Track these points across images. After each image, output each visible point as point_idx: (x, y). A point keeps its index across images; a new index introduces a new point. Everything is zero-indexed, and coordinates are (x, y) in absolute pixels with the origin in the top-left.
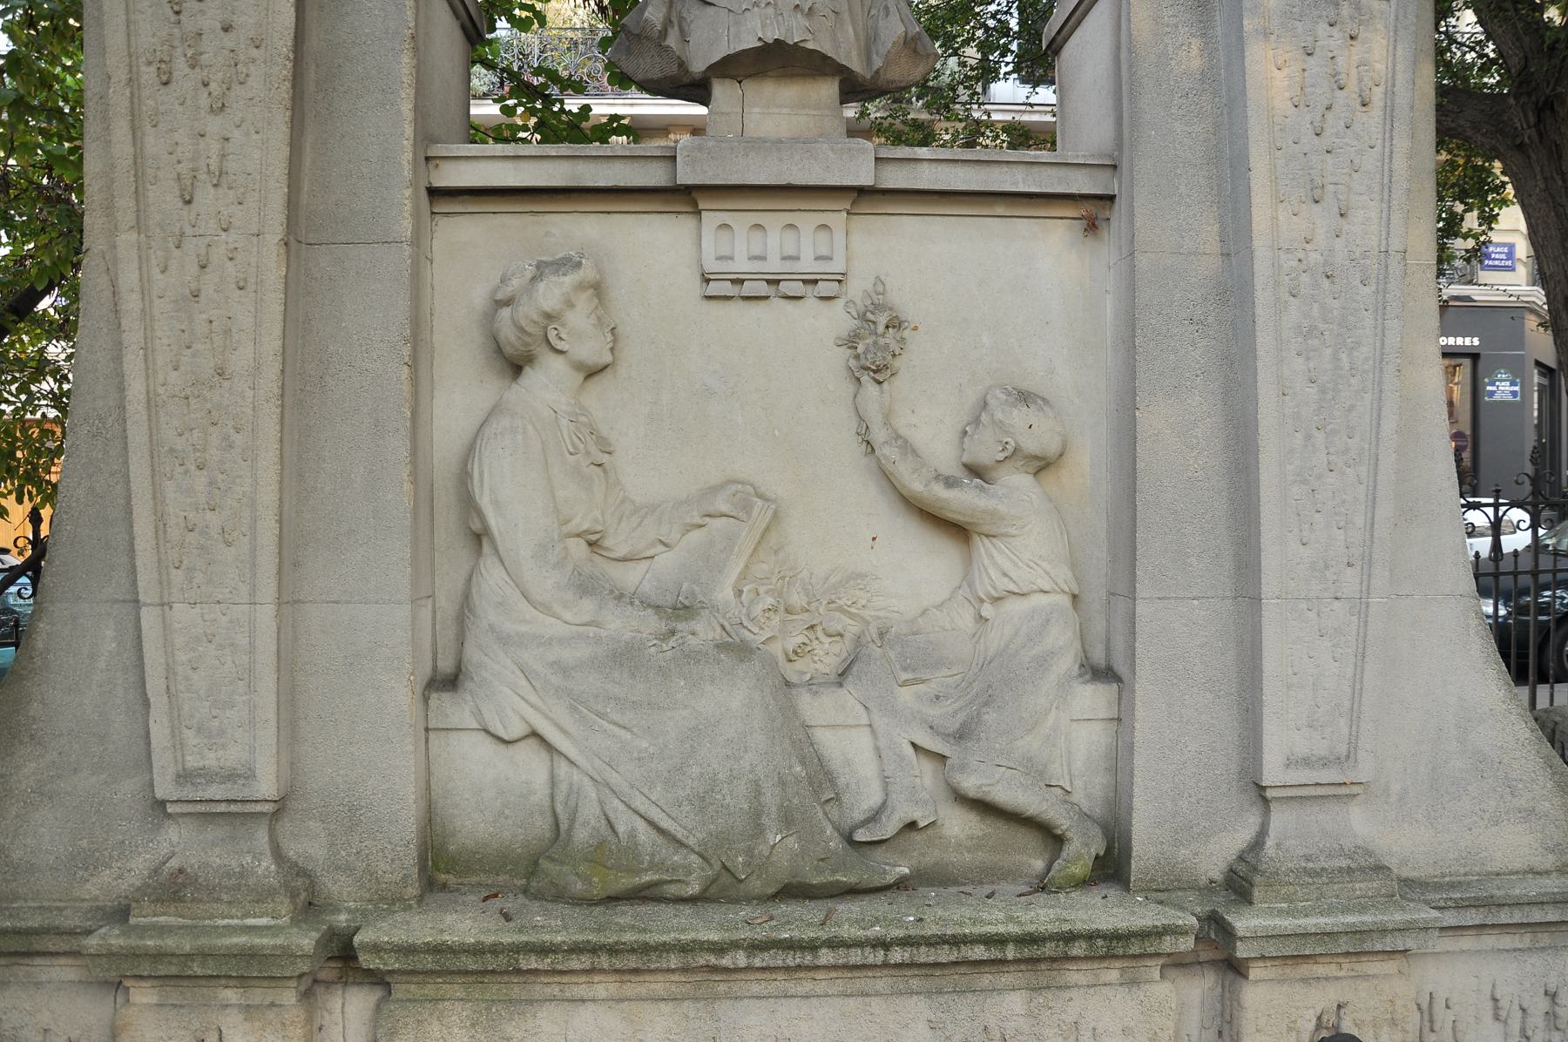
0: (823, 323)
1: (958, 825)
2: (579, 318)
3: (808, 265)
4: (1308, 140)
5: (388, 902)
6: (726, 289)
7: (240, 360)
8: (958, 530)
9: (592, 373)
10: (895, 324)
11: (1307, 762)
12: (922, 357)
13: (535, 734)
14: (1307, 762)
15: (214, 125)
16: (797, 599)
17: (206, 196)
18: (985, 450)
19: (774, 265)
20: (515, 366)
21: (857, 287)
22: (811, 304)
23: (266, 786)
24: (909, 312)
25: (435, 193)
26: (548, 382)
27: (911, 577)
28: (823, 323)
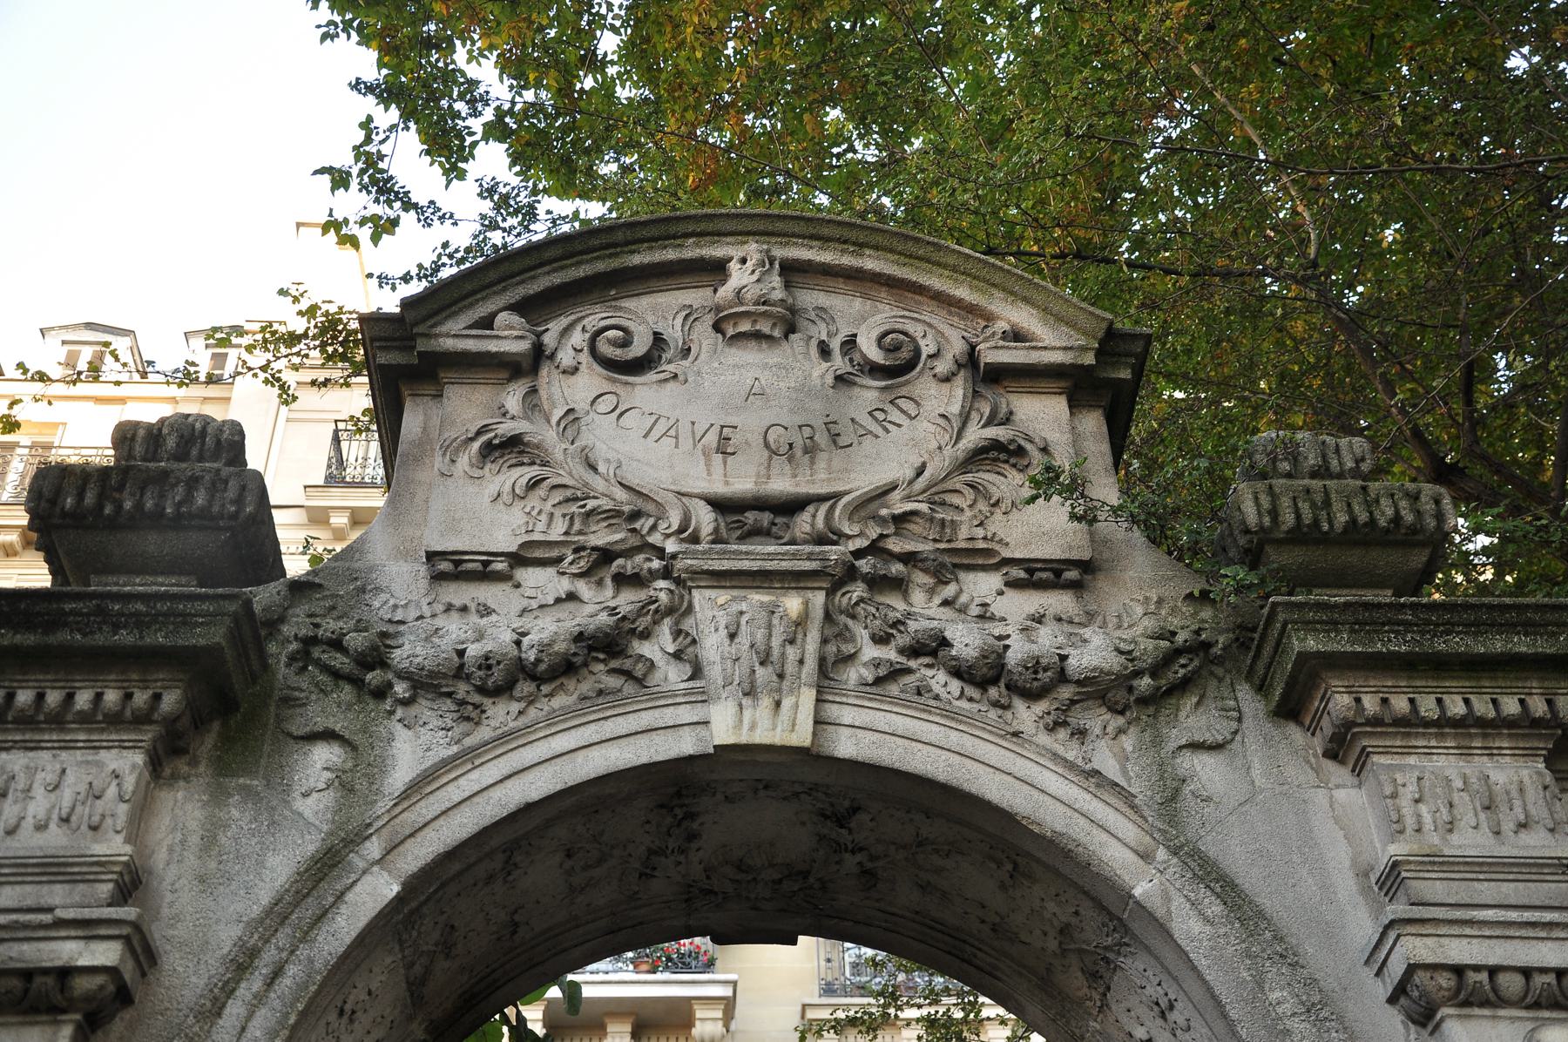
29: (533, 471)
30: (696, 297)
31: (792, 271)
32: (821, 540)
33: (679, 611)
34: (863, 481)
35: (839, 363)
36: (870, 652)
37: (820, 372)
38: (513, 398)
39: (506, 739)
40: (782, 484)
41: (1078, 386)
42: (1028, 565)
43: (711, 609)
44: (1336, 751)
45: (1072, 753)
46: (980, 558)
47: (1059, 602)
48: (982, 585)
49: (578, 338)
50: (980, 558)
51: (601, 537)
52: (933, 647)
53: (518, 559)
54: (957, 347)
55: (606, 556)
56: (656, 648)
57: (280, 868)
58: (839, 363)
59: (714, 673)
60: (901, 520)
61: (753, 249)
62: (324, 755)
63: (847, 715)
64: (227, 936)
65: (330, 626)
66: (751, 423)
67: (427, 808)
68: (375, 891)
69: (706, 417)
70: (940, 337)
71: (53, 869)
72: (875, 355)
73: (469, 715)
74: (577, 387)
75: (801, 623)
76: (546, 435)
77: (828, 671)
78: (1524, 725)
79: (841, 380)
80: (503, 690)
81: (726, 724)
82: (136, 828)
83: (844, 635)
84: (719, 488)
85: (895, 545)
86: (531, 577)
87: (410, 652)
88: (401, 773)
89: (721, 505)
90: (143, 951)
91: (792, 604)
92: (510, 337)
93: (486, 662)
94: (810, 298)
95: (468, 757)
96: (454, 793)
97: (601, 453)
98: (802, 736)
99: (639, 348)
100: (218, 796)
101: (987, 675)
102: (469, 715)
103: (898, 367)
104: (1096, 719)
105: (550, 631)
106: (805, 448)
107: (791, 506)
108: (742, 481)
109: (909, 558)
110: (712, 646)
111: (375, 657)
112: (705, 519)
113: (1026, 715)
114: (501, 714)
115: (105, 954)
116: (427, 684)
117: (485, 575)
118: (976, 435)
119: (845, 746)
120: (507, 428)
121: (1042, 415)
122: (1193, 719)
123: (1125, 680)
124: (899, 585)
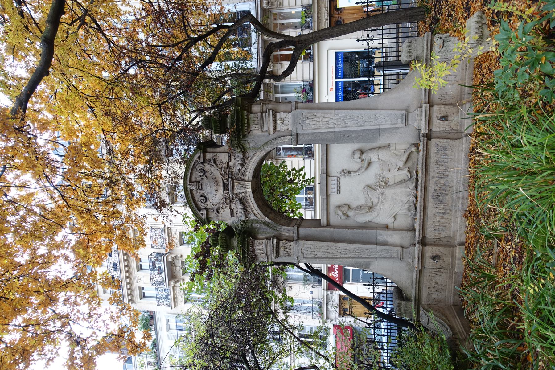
0: (343, 180)
1: (409, 164)
2: (343, 209)
3: (336, 182)
4: (321, 123)
5: (415, 236)
6: (339, 191)
7: (348, 248)
8: (370, 163)
9: (349, 207)
10: (343, 171)
11: (402, 120)
12: (346, 167)
13: (394, 216)
14: (402, 120)
15: (321, 250)
16: (378, 184)
17: (329, 251)
18: (360, 160)
19: (336, 186)
20: (348, 216)
21: (339, 176)
22: (341, 181)
23: (399, 248)
24: (341, 169)
25: (327, 225)
26: (351, 213)
27: (375, 169)
28: (343, 180)
29: (221, 209)
30: (194, 192)
31: (191, 182)
32: (228, 181)
33: (236, 194)
34: (220, 176)
35: (204, 177)
36: (240, 176)
37: (205, 180)
38: (210, 210)
39: (251, 209)
40: (221, 184)
41: (204, 152)
42: (229, 159)
43: (236, 191)
44: (249, 133)
45: (250, 158)
46: (228, 164)
47: (232, 157)
48: (231, 164)
49: (203, 204)
50: (228, 164)
51: (228, 201)
52: (239, 170)
53: (231, 209)
54: (201, 165)
55: (230, 201)
56: (241, 196)
57: (264, 227)
58: (204, 177)
59: (243, 191)
60: (225, 172)
61: (189, 186)
62: (253, 225)
63: (247, 178)
64: (271, 230)
65: (240, 226)
66: (214, 188)
67: (259, 216)
68: (267, 220)
69: (213, 192)
70: (199, 166)
71: (267, 245)
72: (202, 174)
73: (249, 213)
74: (209, 204)
75: (238, 183)
76: (216, 208)
77: (242, 180)
78: (247, 116)
79: (206, 177)
80: (246, 210)
81: (249, 190)
82: (263, 239)
83: (238, 178)
84: (222, 190)
85: (227, 173)
86: (233, 207)
87: (243, 219)
88: (255, 218)
89: (224, 191)
90: (274, 237)
91: (236, 184)
92: (204, 212)
93: (244, 212)
94: (193, 180)
95: (253, 213)
96: (257, 214)
97: (218, 201)
98: (250, 183)
99: (204, 198)
100: (258, 233)
101: (242, 165)
102: (249, 213)
103: (204, 171)
104: (247, 155)
105: (240, 206)
106: (217, 182)
107: (224, 183)
108: (222, 188)
109: (229, 171)
110: (240, 191)
111: (244, 221)
112: (226, 192)
113: (247, 161)
114: (249, 210)
115: (275, 240)
116: (246, 217)
117: (233, 212)
118: (212, 163)
119: (251, 179)
120: (215, 211)
121: (209, 156)
122: (246, 145)
123: (243, 152)
124: (232, 172)
